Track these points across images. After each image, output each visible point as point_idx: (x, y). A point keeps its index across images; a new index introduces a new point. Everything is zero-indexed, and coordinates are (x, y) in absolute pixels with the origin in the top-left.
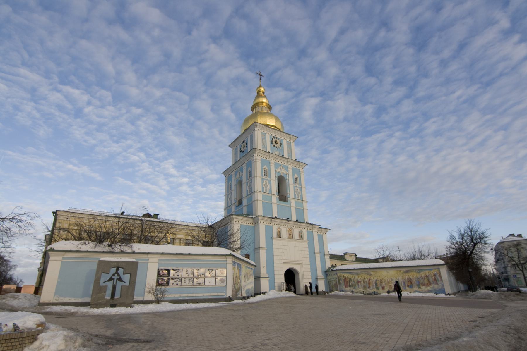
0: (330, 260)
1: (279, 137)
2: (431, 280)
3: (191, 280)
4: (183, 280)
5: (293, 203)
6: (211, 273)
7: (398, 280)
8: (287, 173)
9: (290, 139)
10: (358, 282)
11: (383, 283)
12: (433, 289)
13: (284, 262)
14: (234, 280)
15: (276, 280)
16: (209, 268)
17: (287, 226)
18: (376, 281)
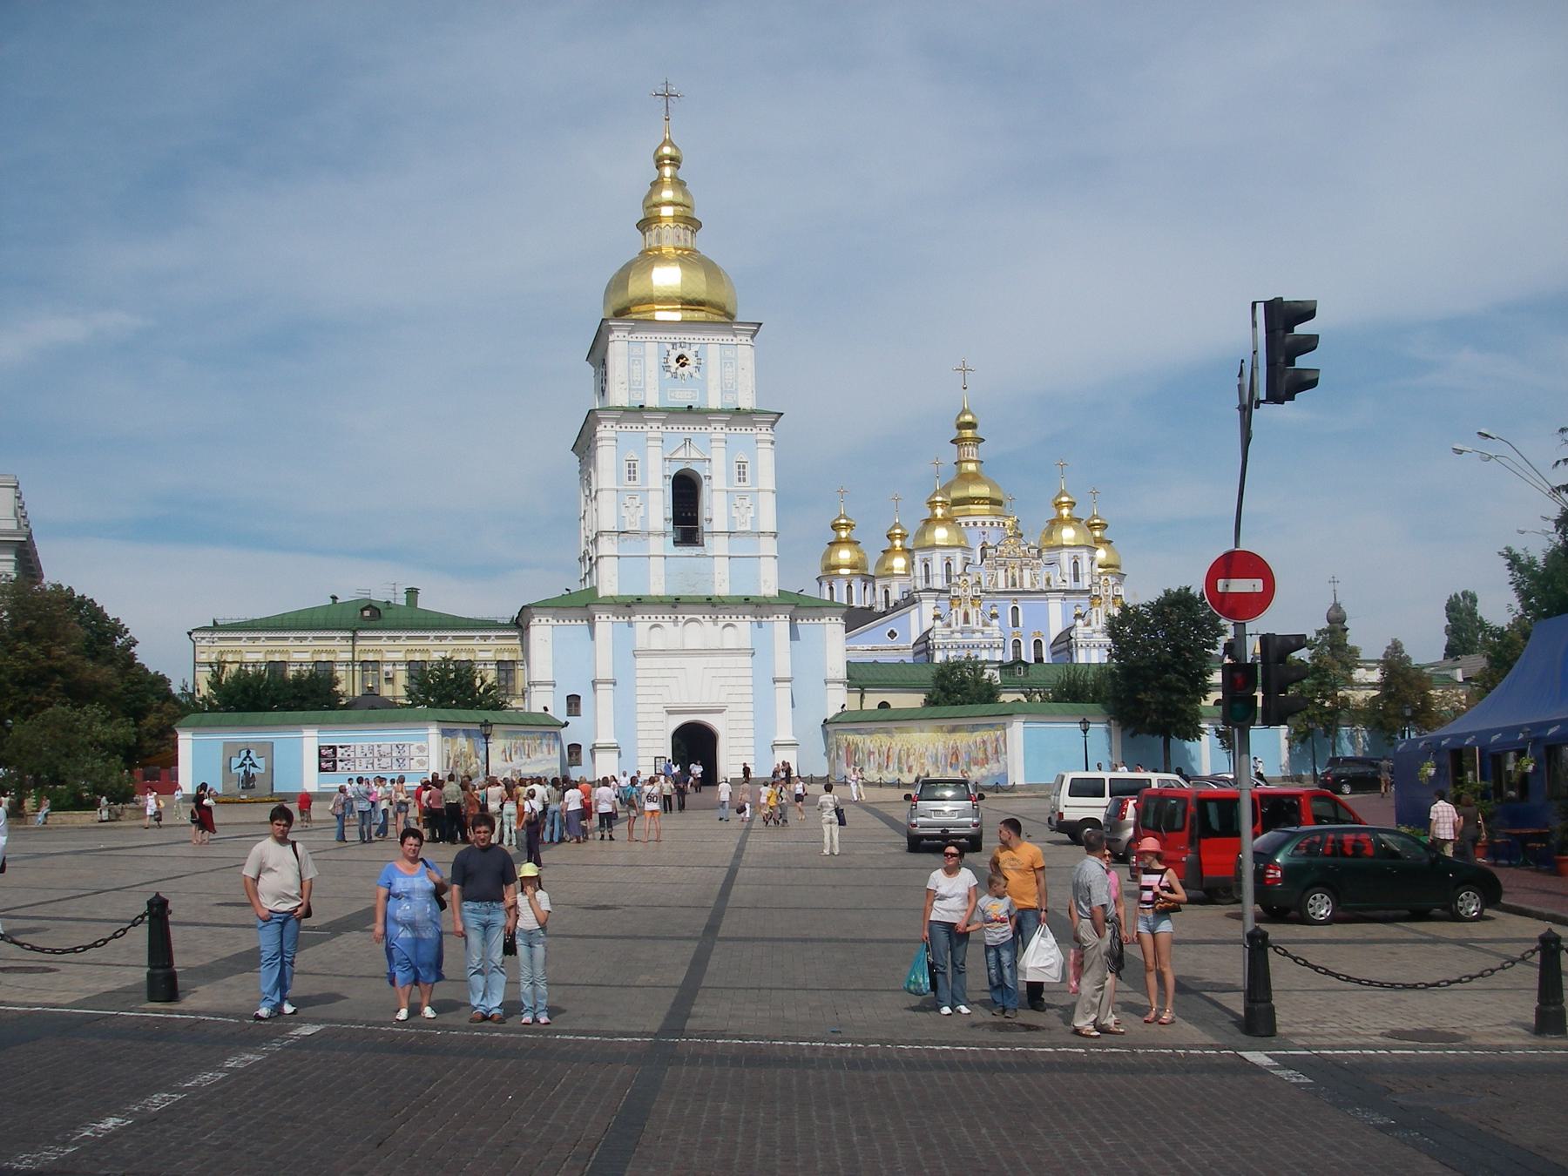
0: (848, 692)
1: (692, 341)
2: (990, 750)
3: (371, 762)
4: (357, 763)
5: (715, 545)
6: (401, 752)
7: (937, 750)
8: (707, 457)
9: (736, 336)
10: (871, 753)
11: (912, 758)
12: (990, 775)
13: (667, 711)
14: (451, 761)
15: (641, 752)
16: (397, 743)
17: (684, 618)
18: (900, 751)
